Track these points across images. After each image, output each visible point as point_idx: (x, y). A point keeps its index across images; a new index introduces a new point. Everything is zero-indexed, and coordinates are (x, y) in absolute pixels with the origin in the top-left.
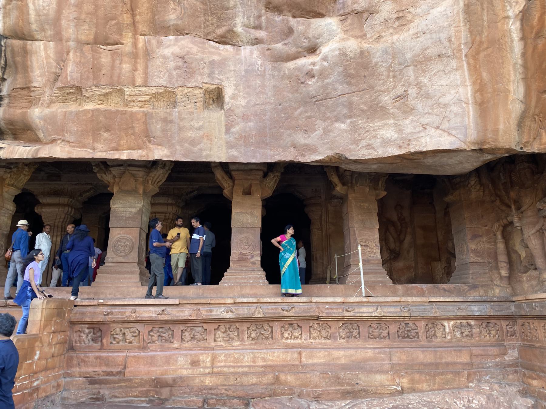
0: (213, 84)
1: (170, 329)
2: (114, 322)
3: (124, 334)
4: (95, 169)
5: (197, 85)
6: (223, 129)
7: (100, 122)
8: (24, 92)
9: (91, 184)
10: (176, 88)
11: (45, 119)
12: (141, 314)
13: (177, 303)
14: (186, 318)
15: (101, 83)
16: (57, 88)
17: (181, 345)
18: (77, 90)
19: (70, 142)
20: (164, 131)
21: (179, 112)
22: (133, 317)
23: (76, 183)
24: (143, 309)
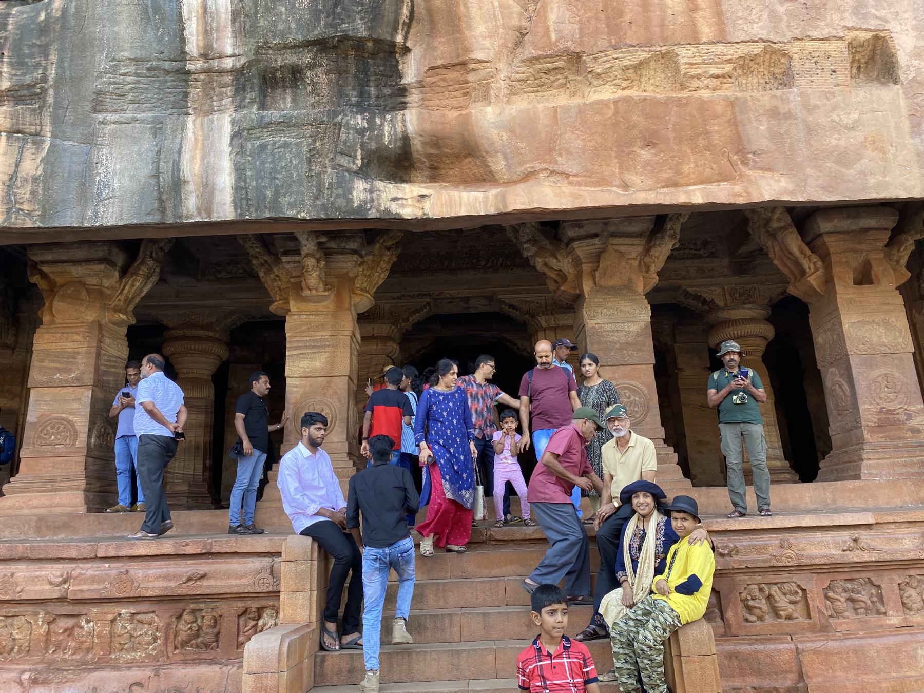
0: (866, 30)
1: (870, 581)
2: (748, 570)
3: (769, 597)
4: (529, 250)
5: (834, 33)
6: (906, 125)
7: (634, 126)
8: (451, 75)
9: (429, 295)
10: (789, 42)
11: (511, 128)
12: (803, 550)
13: (871, 521)
14: (911, 556)
15: (628, 42)
16: (522, 61)
17: (905, 619)
18: (570, 61)
19: (568, 175)
20: (775, 137)
21: (801, 94)
22: (790, 557)
23: (400, 294)
24: (799, 535)
